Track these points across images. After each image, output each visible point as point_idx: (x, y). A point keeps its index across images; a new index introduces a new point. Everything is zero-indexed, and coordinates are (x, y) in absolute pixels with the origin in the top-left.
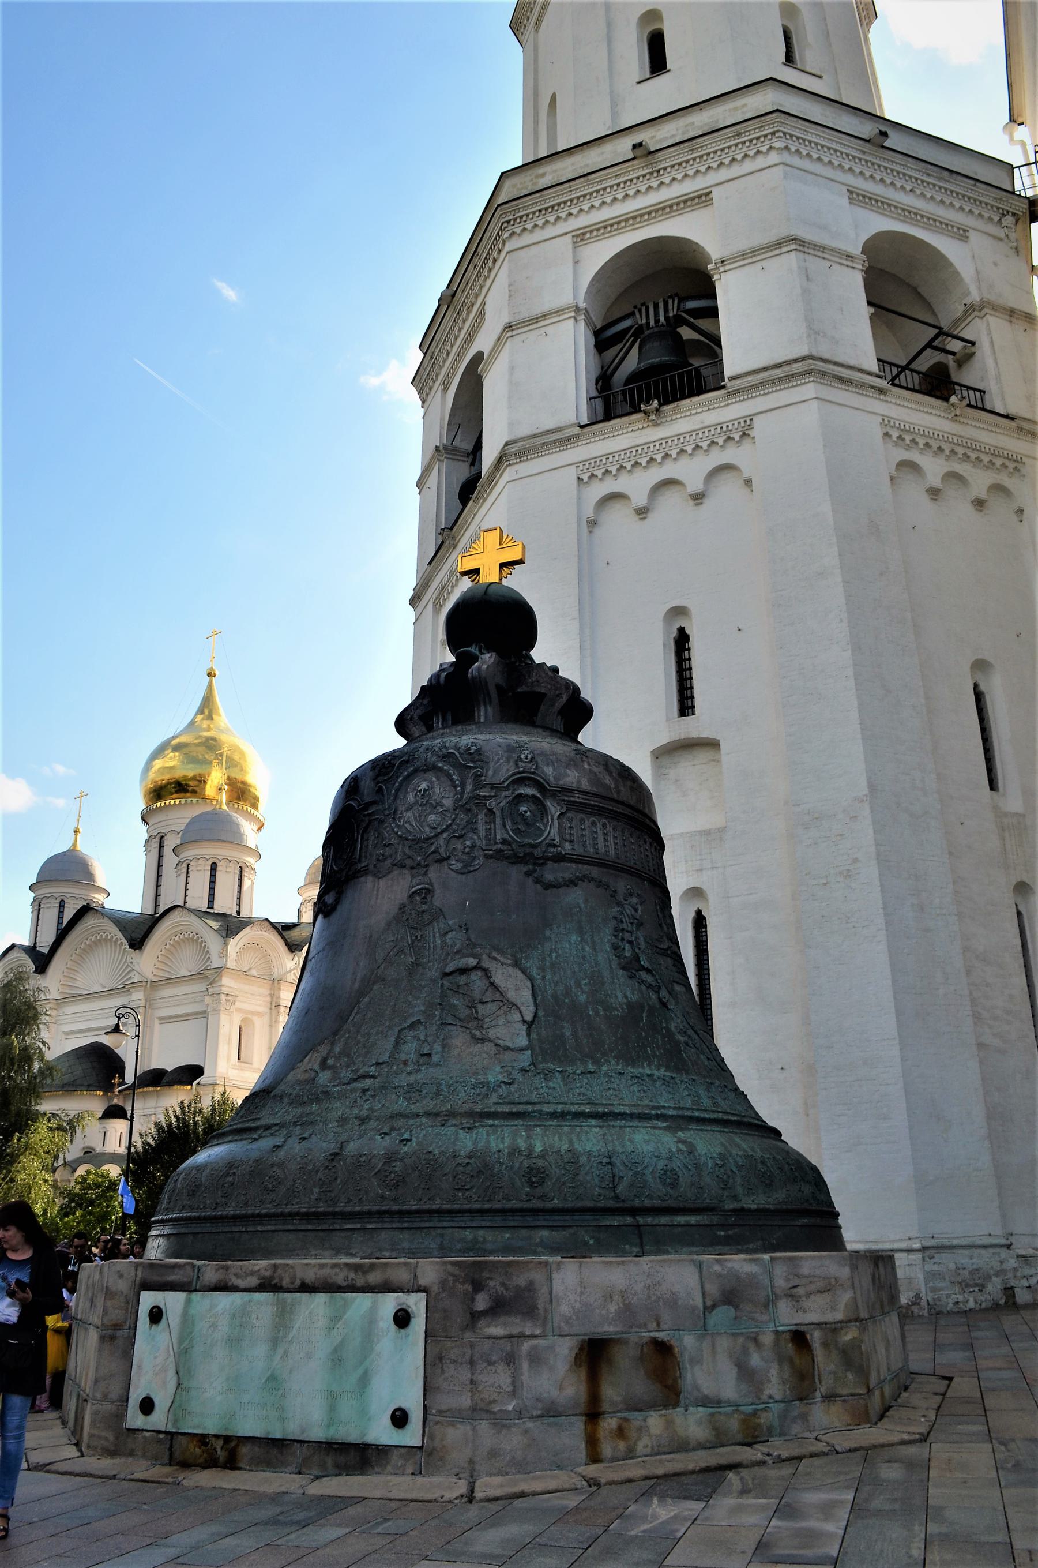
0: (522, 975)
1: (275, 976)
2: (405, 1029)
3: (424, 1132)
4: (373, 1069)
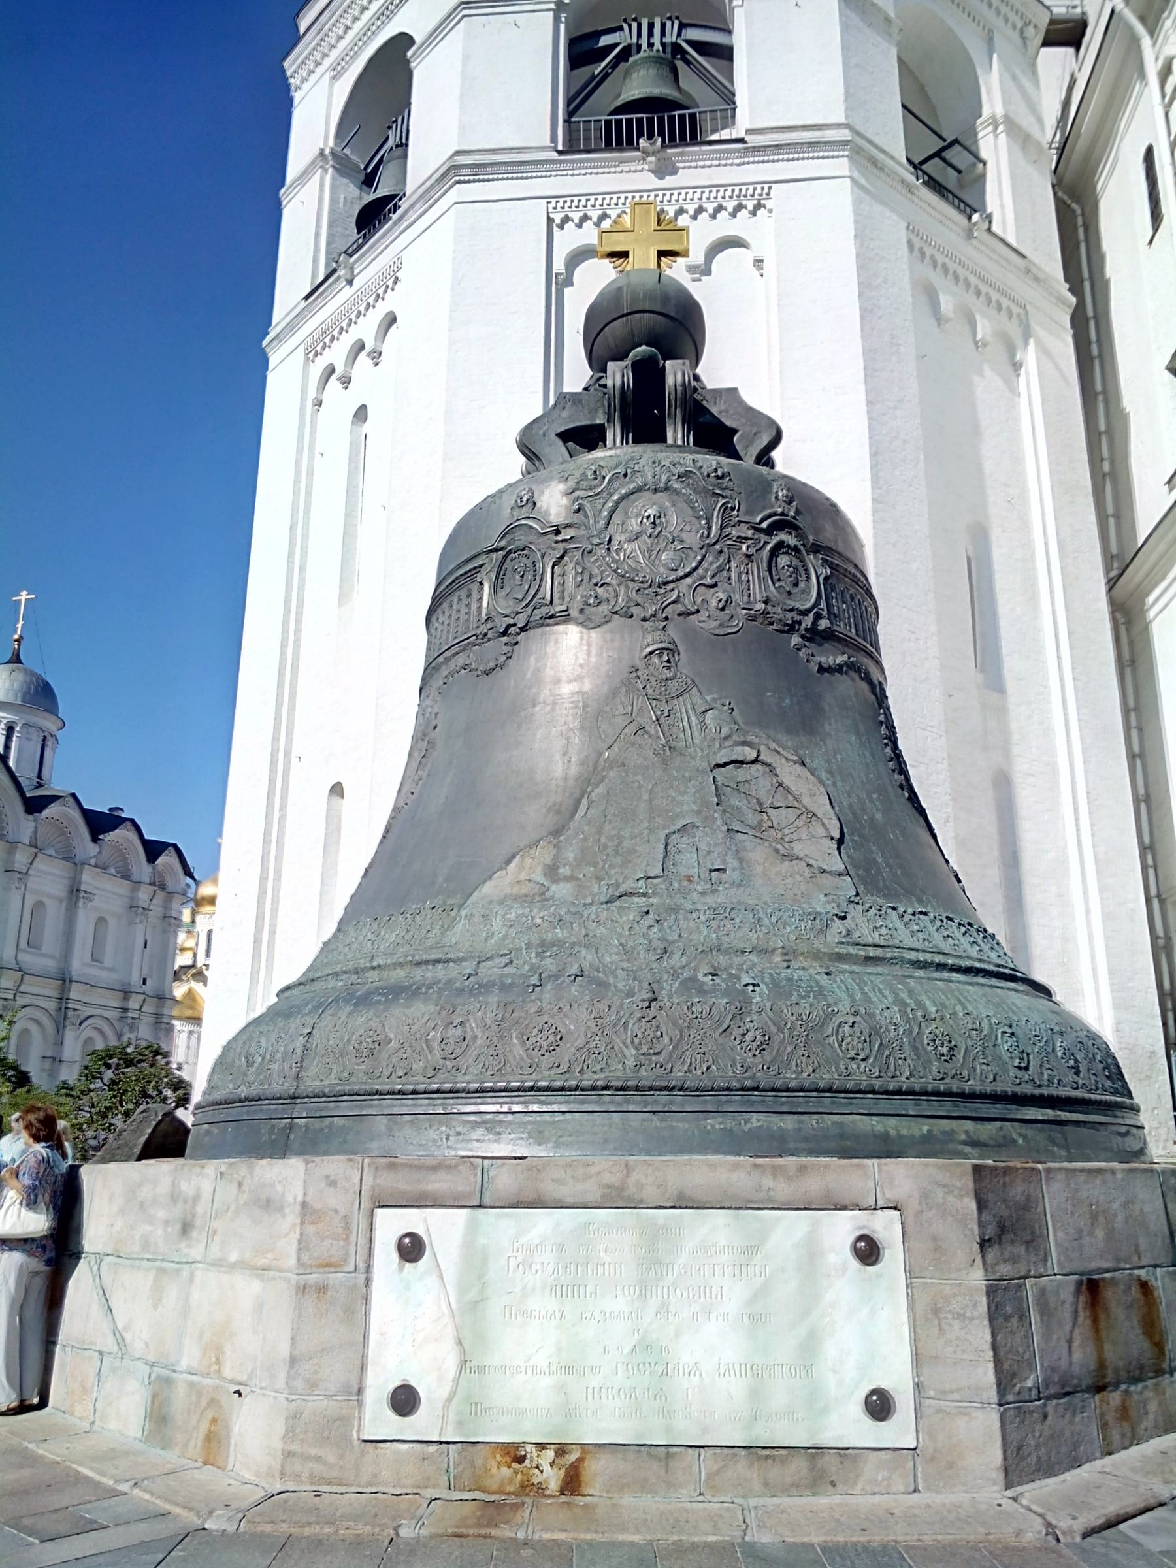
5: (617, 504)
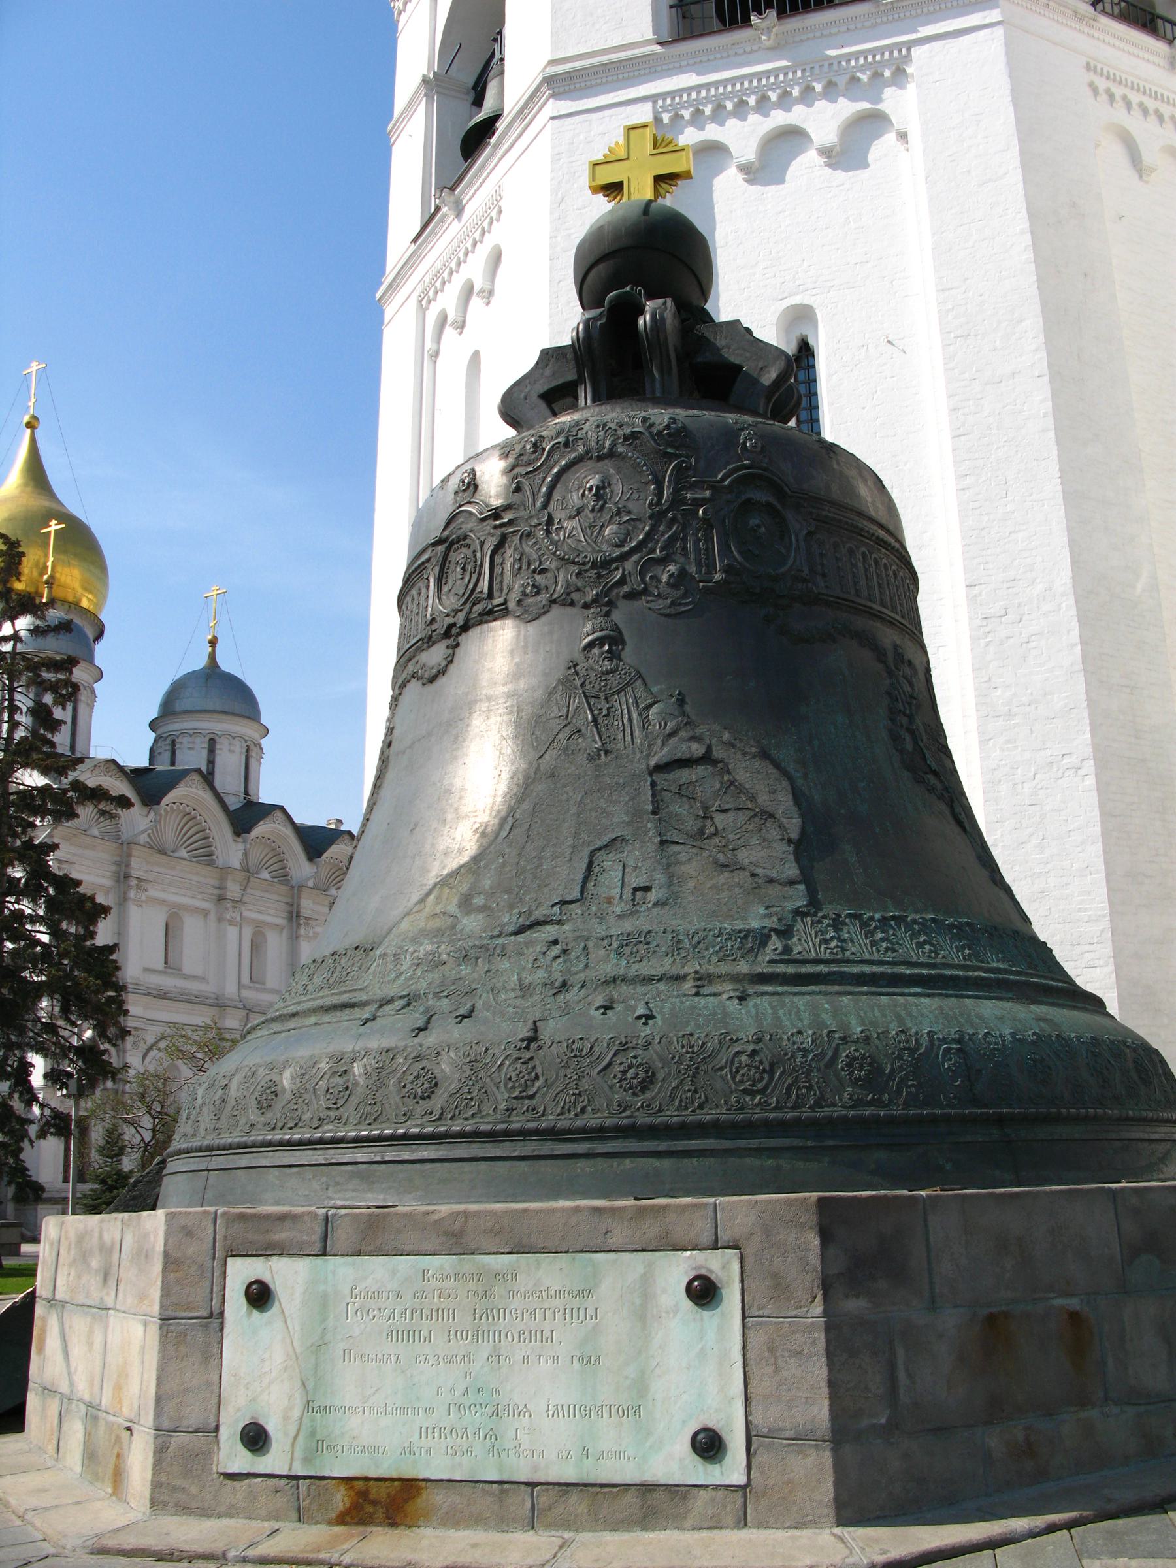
0: (774, 771)
1: (124, 837)
2: (600, 849)
4: (556, 909)
5: (557, 478)
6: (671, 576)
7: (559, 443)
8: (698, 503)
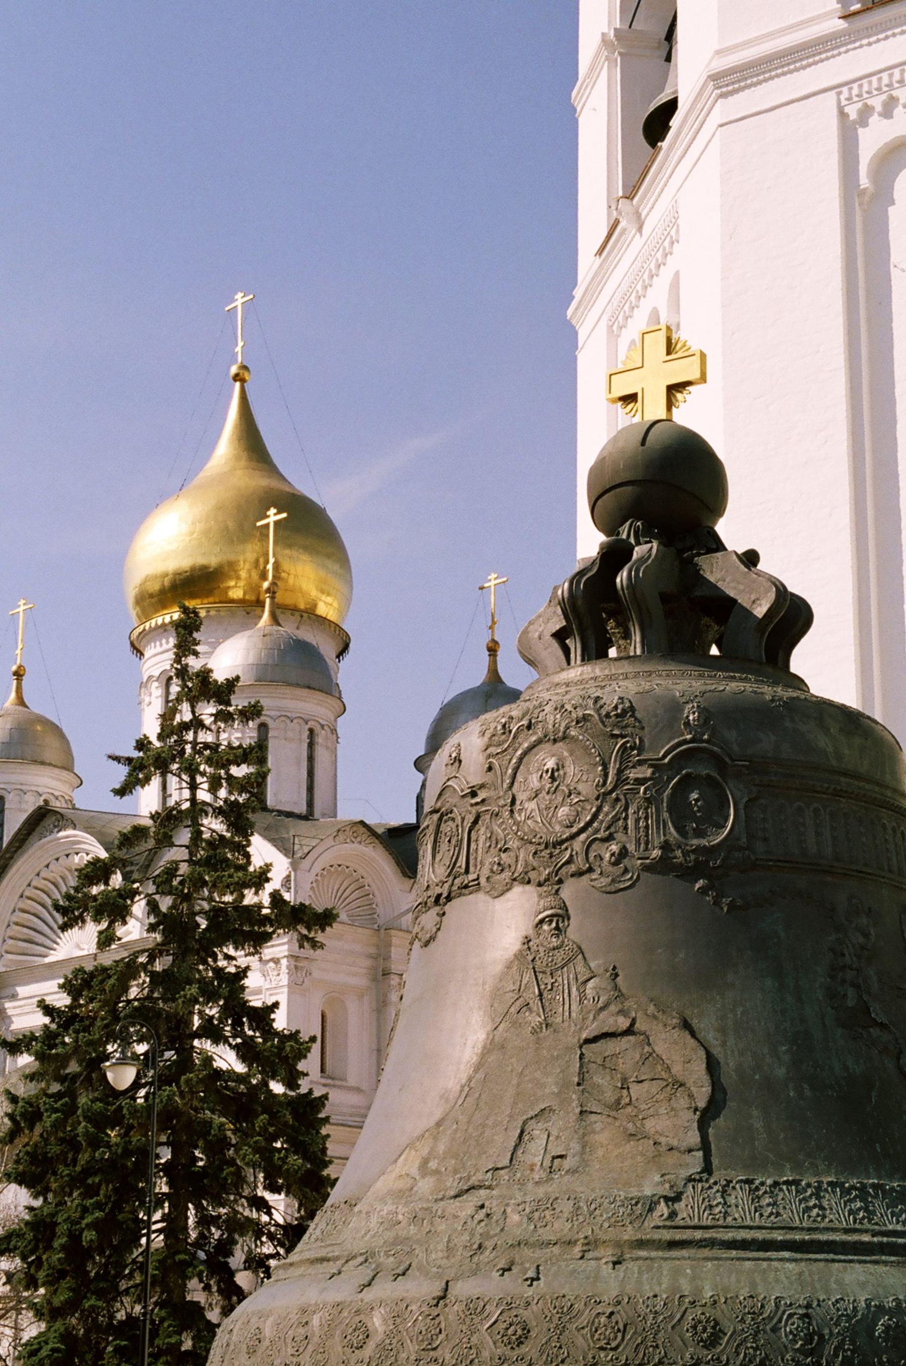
3: (555, 1268)
4: (489, 1174)
5: (521, 759)
6: (613, 855)
7: (523, 725)
8: (639, 782)
